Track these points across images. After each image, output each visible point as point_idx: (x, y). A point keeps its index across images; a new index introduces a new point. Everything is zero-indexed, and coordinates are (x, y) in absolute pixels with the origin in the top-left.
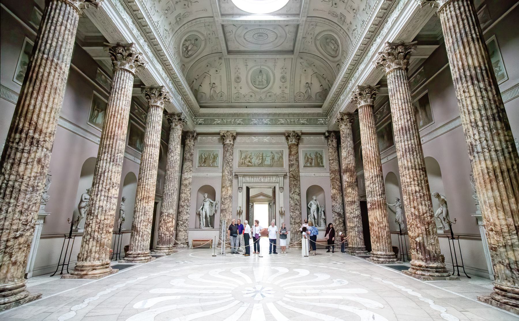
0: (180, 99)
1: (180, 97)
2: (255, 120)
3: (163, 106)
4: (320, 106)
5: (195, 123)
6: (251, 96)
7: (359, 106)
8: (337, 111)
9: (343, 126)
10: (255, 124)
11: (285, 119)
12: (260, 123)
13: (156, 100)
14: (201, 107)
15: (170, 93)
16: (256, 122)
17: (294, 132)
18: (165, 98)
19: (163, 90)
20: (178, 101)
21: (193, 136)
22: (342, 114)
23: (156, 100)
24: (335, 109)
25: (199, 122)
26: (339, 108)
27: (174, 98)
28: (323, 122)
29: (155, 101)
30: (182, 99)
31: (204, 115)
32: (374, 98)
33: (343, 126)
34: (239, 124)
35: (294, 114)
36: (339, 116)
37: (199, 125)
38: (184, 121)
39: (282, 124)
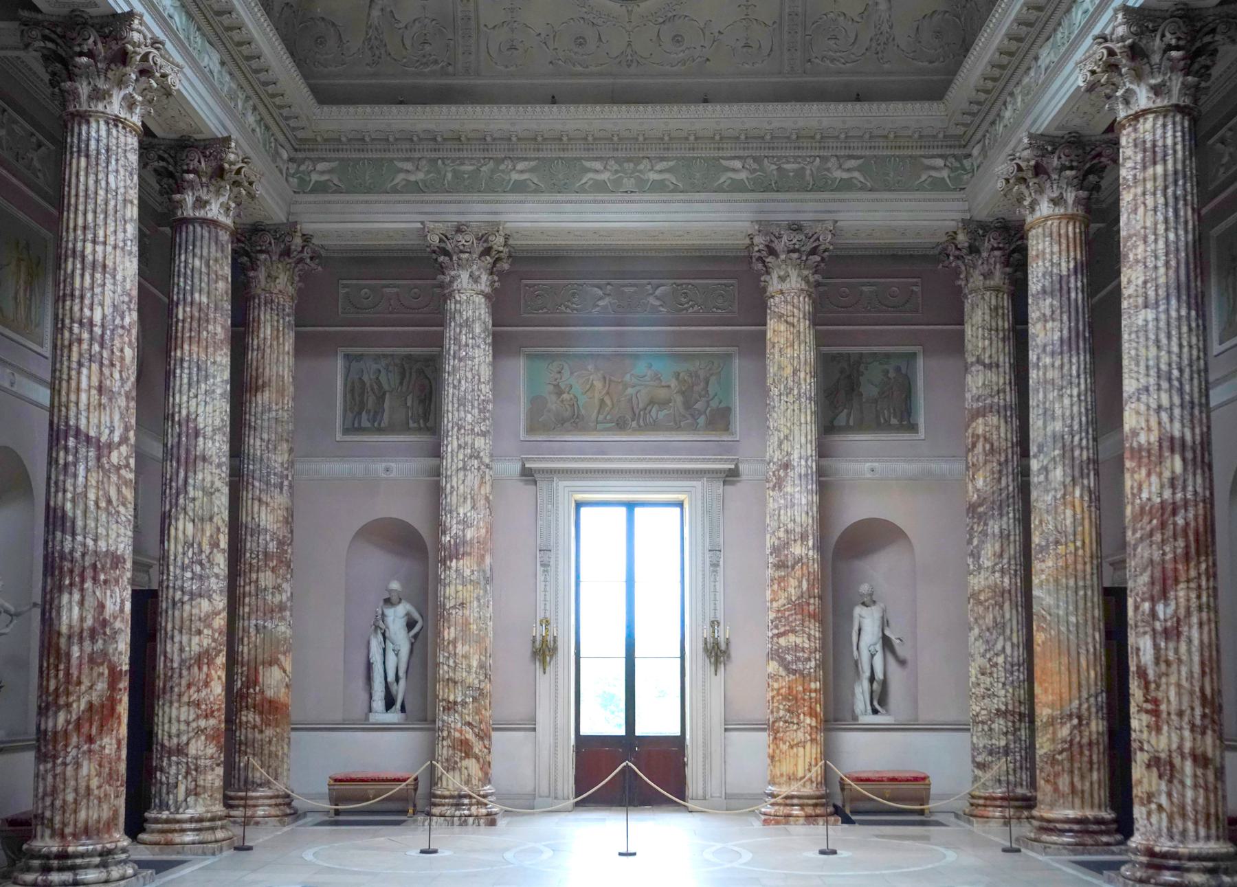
0: (216, 67)
1: (216, 57)
2: (597, 165)
3: (136, 119)
4: (935, 92)
5: (294, 181)
6: (581, 41)
7: (1122, 113)
8: (1017, 124)
9: (1045, 208)
10: (600, 187)
11: (755, 159)
12: (629, 183)
13: (102, 85)
14: (324, 96)
15: (168, 45)
16: (605, 176)
17: (796, 227)
18: (144, 73)
19: (136, 36)
20: (205, 75)
21: (287, 253)
22: (1045, 144)
23: (102, 85)
24: (1007, 114)
25: (315, 177)
26: (1028, 110)
27: (187, 70)
28: (945, 174)
29: (96, 89)
30: (223, 63)
31: (334, 142)
32: (1204, 72)
33: (1045, 208)
34: (519, 187)
35: (800, 138)
36: (1026, 154)
37: (312, 191)
38: (236, 184)
39: (737, 187)
